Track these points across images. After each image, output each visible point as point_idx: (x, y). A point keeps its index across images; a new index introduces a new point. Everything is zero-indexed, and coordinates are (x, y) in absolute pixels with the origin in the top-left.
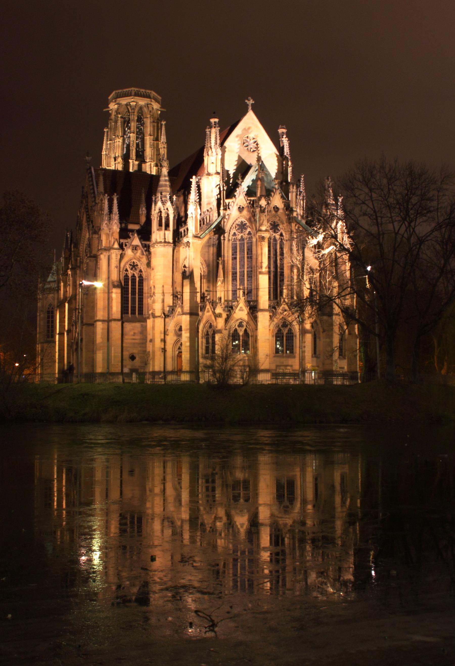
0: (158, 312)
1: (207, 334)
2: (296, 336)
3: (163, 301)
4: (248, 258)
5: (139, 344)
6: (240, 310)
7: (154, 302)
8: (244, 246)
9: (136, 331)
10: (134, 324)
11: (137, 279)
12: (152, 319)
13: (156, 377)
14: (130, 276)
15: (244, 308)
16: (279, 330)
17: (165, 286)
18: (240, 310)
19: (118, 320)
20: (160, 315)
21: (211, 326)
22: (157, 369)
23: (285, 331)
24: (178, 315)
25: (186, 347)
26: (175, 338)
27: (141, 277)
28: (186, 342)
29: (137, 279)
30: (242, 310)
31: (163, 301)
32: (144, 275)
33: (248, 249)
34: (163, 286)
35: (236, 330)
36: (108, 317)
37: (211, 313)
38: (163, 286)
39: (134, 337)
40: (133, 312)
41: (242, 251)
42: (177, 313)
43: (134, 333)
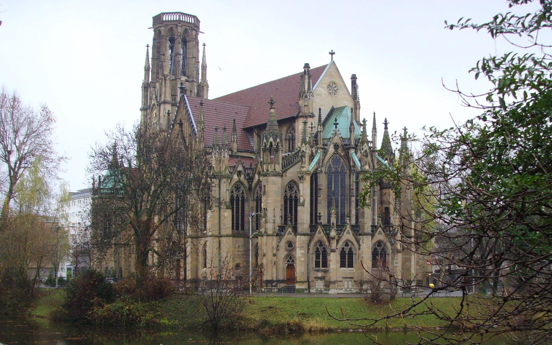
0: (270, 232)
1: (317, 251)
2: (388, 254)
3: (274, 222)
4: (341, 188)
5: (242, 255)
6: (347, 233)
7: (266, 222)
8: (338, 178)
9: (241, 245)
10: (238, 239)
11: (240, 199)
12: (265, 237)
13: (269, 285)
15: (350, 231)
16: (375, 249)
18: (347, 233)
19: (220, 233)
20: (271, 233)
21: (321, 245)
22: (269, 278)
24: (288, 234)
25: (300, 261)
26: (286, 253)
27: (243, 197)
28: (300, 257)
29: (240, 199)
31: (274, 222)
32: (245, 196)
33: (342, 181)
34: (274, 209)
36: (220, 233)
37: (322, 234)
38: (274, 209)
39: (239, 250)
40: (237, 228)
41: (336, 182)
42: (287, 232)
43: (239, 246)
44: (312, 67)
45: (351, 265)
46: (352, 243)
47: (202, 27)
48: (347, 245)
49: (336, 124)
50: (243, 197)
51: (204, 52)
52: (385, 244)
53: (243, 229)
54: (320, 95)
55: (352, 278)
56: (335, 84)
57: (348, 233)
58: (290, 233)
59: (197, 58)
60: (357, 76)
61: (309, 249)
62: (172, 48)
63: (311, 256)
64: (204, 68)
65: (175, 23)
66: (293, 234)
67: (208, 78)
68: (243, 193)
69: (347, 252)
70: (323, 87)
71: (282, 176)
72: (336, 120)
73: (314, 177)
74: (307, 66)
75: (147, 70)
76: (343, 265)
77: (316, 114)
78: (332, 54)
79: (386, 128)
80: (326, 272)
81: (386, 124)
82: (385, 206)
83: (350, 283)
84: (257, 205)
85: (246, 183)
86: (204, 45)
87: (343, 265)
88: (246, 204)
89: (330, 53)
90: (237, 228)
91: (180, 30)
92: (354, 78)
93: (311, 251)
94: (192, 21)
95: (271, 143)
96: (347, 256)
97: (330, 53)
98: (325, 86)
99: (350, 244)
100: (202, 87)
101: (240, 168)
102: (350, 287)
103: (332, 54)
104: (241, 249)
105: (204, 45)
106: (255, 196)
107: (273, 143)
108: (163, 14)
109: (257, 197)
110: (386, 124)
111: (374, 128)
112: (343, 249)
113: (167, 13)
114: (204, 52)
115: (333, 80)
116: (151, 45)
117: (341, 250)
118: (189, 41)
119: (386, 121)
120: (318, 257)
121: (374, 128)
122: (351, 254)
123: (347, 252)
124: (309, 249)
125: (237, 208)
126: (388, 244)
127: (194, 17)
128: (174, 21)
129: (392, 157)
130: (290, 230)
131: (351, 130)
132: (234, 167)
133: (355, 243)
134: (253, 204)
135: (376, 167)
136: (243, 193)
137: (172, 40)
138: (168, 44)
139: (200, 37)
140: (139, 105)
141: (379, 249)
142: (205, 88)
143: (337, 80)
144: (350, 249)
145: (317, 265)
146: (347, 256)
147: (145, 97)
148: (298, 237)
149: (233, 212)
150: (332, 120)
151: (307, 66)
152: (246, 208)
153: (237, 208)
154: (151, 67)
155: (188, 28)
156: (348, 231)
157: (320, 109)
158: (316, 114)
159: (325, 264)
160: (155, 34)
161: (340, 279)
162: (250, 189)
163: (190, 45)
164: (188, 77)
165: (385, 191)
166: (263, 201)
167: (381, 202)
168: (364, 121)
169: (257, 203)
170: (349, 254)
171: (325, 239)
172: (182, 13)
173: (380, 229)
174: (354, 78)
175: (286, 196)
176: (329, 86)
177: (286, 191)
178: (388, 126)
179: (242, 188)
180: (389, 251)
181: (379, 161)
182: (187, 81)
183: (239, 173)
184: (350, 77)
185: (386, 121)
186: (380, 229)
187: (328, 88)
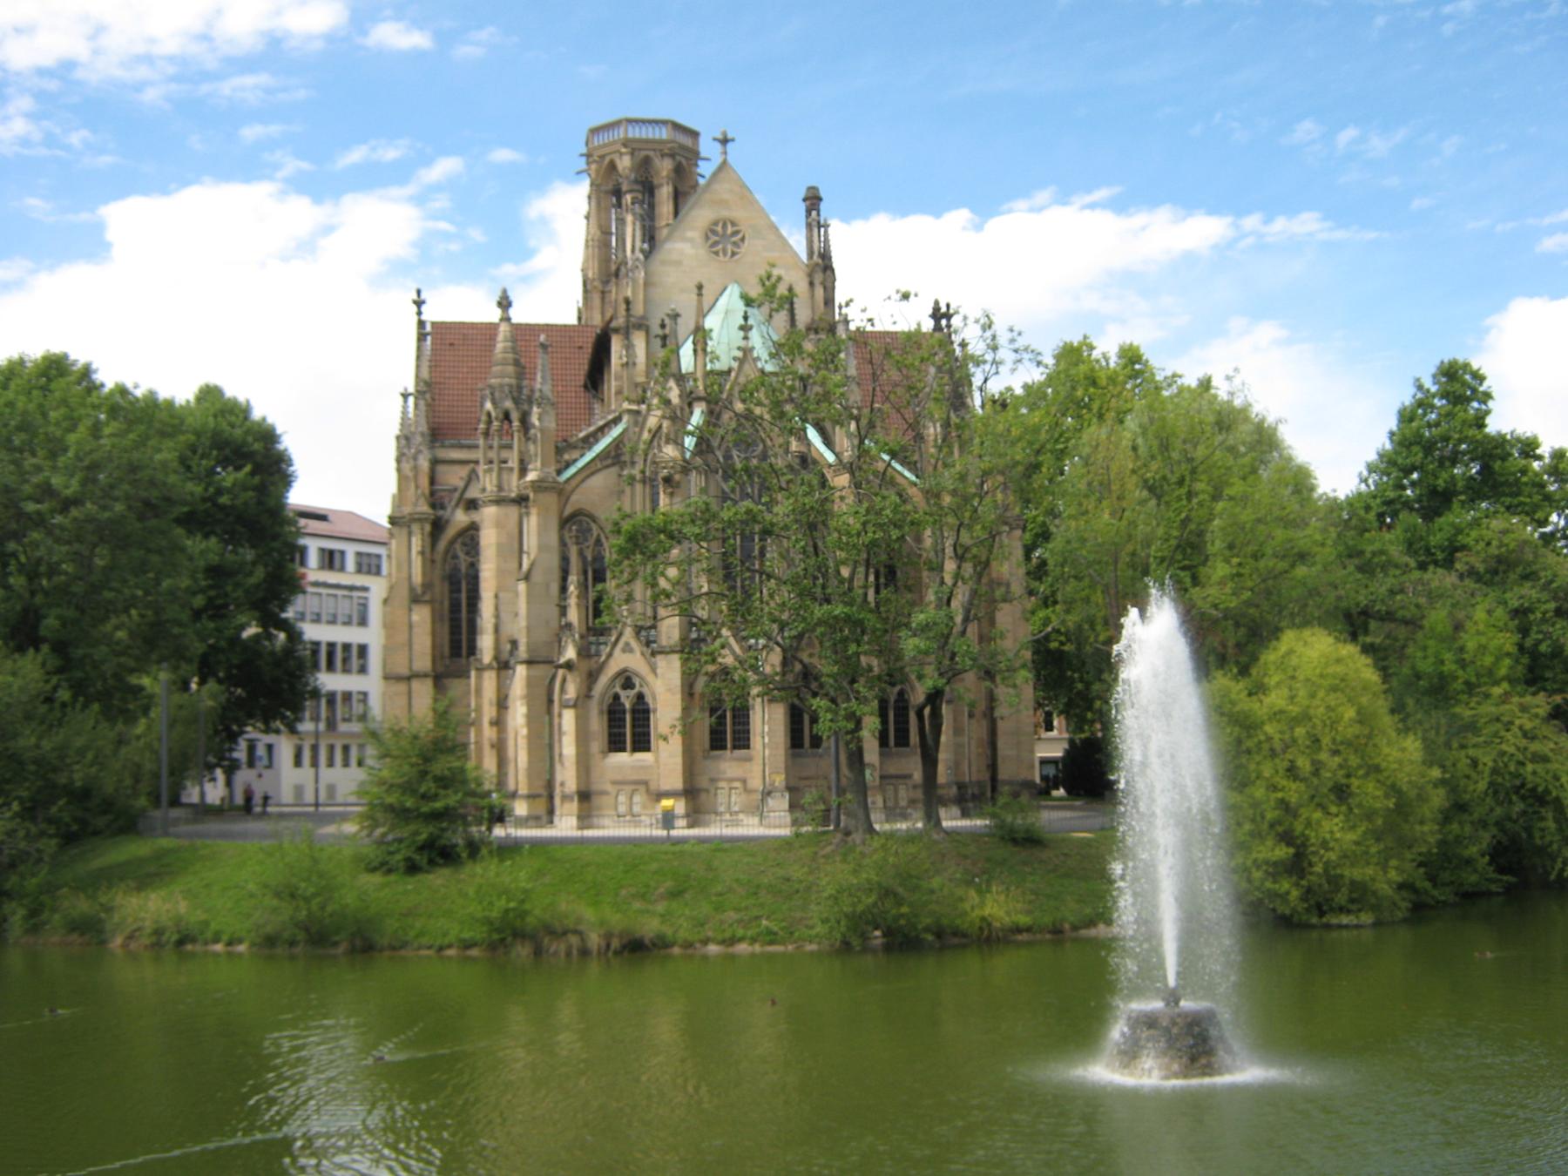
14: (463, 568)
15: (634, 644)
17: (501, 595)
18: (624, 651)
30: (631, 651)
35: (616, 697)
38: (496, 596)
46: (642, 678)
54: (678, 263)
55: (646, 783)
56: (733, 224)
57: (628, 649)
60: (822, 194)
69: (628, 706)
70: (691, 240)
76: (616, 744)
91: (625, 163)
95: (489, 414)
96: (628, 717)
99: (637, 681)
103: (725, 141)
115: (725, 213)
117: (608, 700)
123: (628, 706)
143: (737, 214)
144: (640, 697)
146: (628, 717)
155: (651, 154)
156: (627, 644)
170: (634, 711)
172: (630, 121)
184: (802, 194)
187: (707, 238)
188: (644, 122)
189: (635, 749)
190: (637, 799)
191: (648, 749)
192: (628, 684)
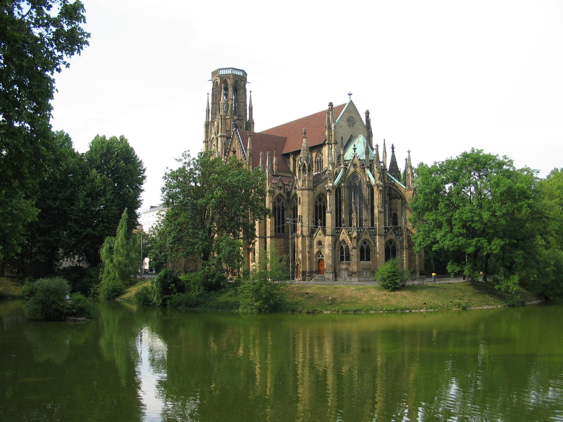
2: (398, 250)
23: (391, 247)
27: (283, 207)
32: (285, 206)
35: (362, 246)
37: (346, 234)
44: (335, 105)
45: (368, 259)
47: (249, 79)
48: (365, 243)
49: (355, 149)
50: (283, 207)
51: (251, 98)
52: (395, 242)
53: (283, 231)
54: (342, 127)
55: (370, 269)
57: (366, 233)
58: (320, 235)
59: (245, 102)
61: (335, 247)
62: (226, 95)
63: (337, 252)
64: (251, 109)
65: (229, 76)
66: (323, 235)
67: (254, 117)
68: (283, 203)
70: (343, 121)
71: (313, 190)
72: (355, 146)
73: (338, 190)
74: (331, 104)
75: (208, 111)
76: (362, 259)
77: (339, 141)
78: (350, 95)
79: (393, 151)
80: (349, 264)
81: (393, 148)
82: (393, 212)
83: (368, 273)
84: (294, 213)
85: (285, 196)
86: (251, 92)
87: (362, 259)
88: (285, 212)
89: (349, 94)
90: (279, 231)
92: (367, 113)
93: (337, 248)
94: (241, 74)
95: (304, 164)
97: (349, 94)
98: (345, 119)
99: (367, 242)
100: (250, 124)
101: (280, 185)
102: (368, 276)
103: (350, 95)
104: (282, 247)
105: (251, 92)
106: (293, 206)
107: (306, 165)
108: (220, 69)
109: (294, 207)
110: (393, 148)
111: (385, 151)
112: (362, 246)
113: (222, 69)
114: (251, 98)
115: (351, 115)
116: (210, 92)
118: (239, 89)
119: (393, 146)
120: (342, 253)
121: (385, 151)
122: (368, 250)
124: (335, 247)
125: (279, 215)
126: (398, 242)
127: (243, 71)
128: (227, 74)
129: (398, 174)
130: (320, 232)
131: (367, 153)
132: (276, 183)
133: (372, 242)
134: (291, 212)
135: (387, 182)
136: (283, 203)
137: (226, 89)
138: (223, 92)
139: (247, 86)
140: (203, 138)
141: (391, 247)
142: (252, 124)
144: (368, 246)
145: (342, 259)
147: (207, 132)
148: (327, 237)
149: (275, 219)
150: (352, 147)
151: (331, 104)
152: (285, 215)
153: (279, 215)
154: (210, 109)
157: (342, 138)
158: (339, 141)
159: (348, 259)
160: (213, 85)
161: (361, 270)
162: (288, 201)
163: (240, 92)
164: (239, 116)
165: (393, 201)
166: (299, 209)
167: (390, 210)
168: (377, 146)
169: (294, 211)
171: (348, 238)
172: (233, 69)
173: (391, 230)
174: (367, 113)
175: (316, 206)
176: (348, 120)
177: (316, 202)
178: (395, 150)
179: (282, 200)
180: (398, 247)
181: (388, 177)
182: (238, 119)
183: (280, 188)
184: (365, 112)
185: (393, 146)
186: (391, 230)
188: (237, 69)
189: (367, 260)
190: (368, 273)
191: (369, 260)
192: (365, 243)
